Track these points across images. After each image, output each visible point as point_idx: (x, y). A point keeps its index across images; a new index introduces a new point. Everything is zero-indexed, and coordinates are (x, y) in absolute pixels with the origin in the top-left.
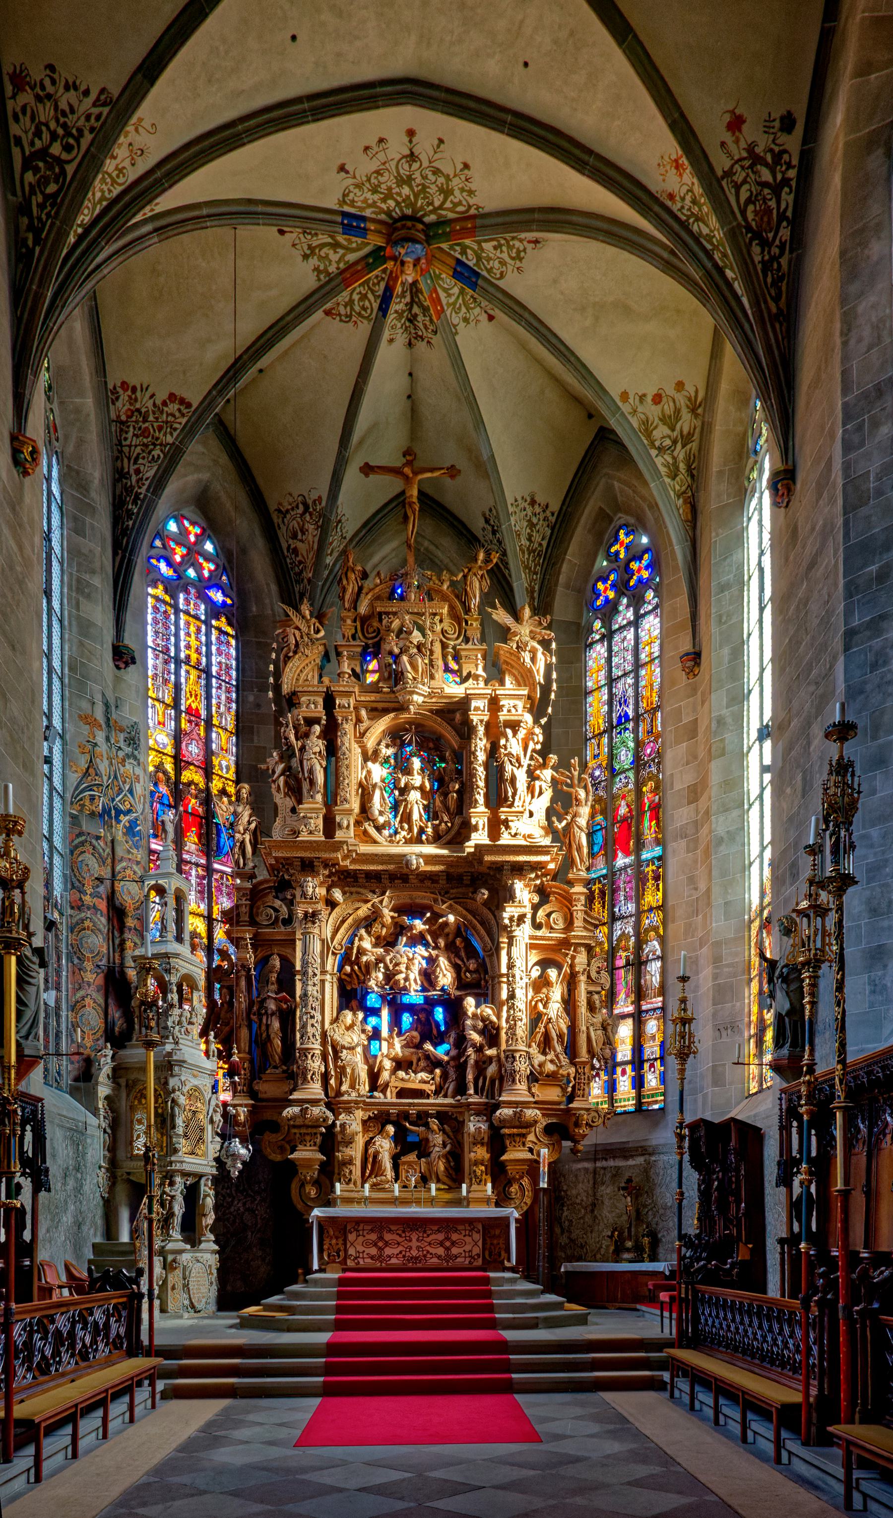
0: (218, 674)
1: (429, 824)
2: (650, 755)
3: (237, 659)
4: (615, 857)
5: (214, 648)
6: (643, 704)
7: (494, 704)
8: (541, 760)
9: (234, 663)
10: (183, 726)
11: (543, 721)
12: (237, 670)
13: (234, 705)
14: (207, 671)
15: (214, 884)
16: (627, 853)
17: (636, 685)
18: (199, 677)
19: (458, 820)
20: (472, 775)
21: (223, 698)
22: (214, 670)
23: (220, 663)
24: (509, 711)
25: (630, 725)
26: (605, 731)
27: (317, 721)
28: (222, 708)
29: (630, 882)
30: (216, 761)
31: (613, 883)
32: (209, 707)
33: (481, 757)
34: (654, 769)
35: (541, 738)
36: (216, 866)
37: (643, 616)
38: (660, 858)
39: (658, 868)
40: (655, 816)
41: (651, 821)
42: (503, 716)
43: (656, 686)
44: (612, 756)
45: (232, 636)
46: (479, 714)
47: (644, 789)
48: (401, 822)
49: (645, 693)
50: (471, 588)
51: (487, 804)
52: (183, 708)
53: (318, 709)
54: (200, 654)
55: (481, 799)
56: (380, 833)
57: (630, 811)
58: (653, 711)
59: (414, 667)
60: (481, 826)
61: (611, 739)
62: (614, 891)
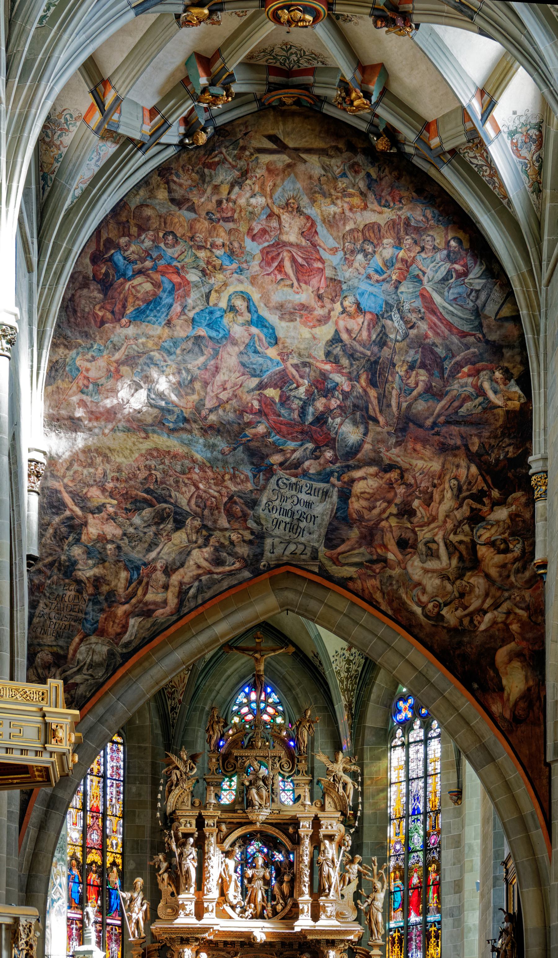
0: (112, 776)
1: (269, 904)
2: (434, 844)
3: (124, 761)
4: (409, 915)
5: (108, 757)
6: (430, 805)
7: (316, 823)
8: (350, 857)
9: (122, 763)
10: (88, 822)
11: (352, 831)
12: (124, 769)
13: (122, 796)
14: (104, 777)
15: (107, 935)
16: (418, 914)
17: (425, 788)
18: (99, 782)
19: (290, 902)
20: (301, 872)
21: (114, 793)
22: (109, 773)
23: (112, 767)
24: (327, 828)
25: (421, 817)
26: (403, 817)
27: (191, 835)
28: (114, 800)
29: (419, 936)
30: (109, 842)
31: (408, 934)
32: (105, 804)
33: (306, 860)
34: (436, 855)
35: (350, 842)
36: (109, 921)
37: (431, 738)
38: (439, 923)
39: (438, 929)
40: (438, 891)
41: (434, 894)
42: (323, 832)
43: (438, 794)
44: (408, 838)
45: (121, 744)
46: (306, 828)
47: (430, 869)
48: (249, 903)
49: (431, 797)
50: (302, 736)
51: (311, 893)
52: (88, 809)
53: (192, 828)
54: (99, 765)
55: (306, 890)
56: (234, 911)
57: (420, 882)
58: (437, 812)
59: (261, 797)
60: (306, 910)
61: (407, 824)
62: (409, 940)
